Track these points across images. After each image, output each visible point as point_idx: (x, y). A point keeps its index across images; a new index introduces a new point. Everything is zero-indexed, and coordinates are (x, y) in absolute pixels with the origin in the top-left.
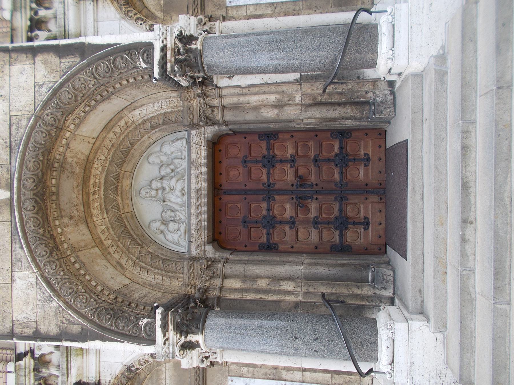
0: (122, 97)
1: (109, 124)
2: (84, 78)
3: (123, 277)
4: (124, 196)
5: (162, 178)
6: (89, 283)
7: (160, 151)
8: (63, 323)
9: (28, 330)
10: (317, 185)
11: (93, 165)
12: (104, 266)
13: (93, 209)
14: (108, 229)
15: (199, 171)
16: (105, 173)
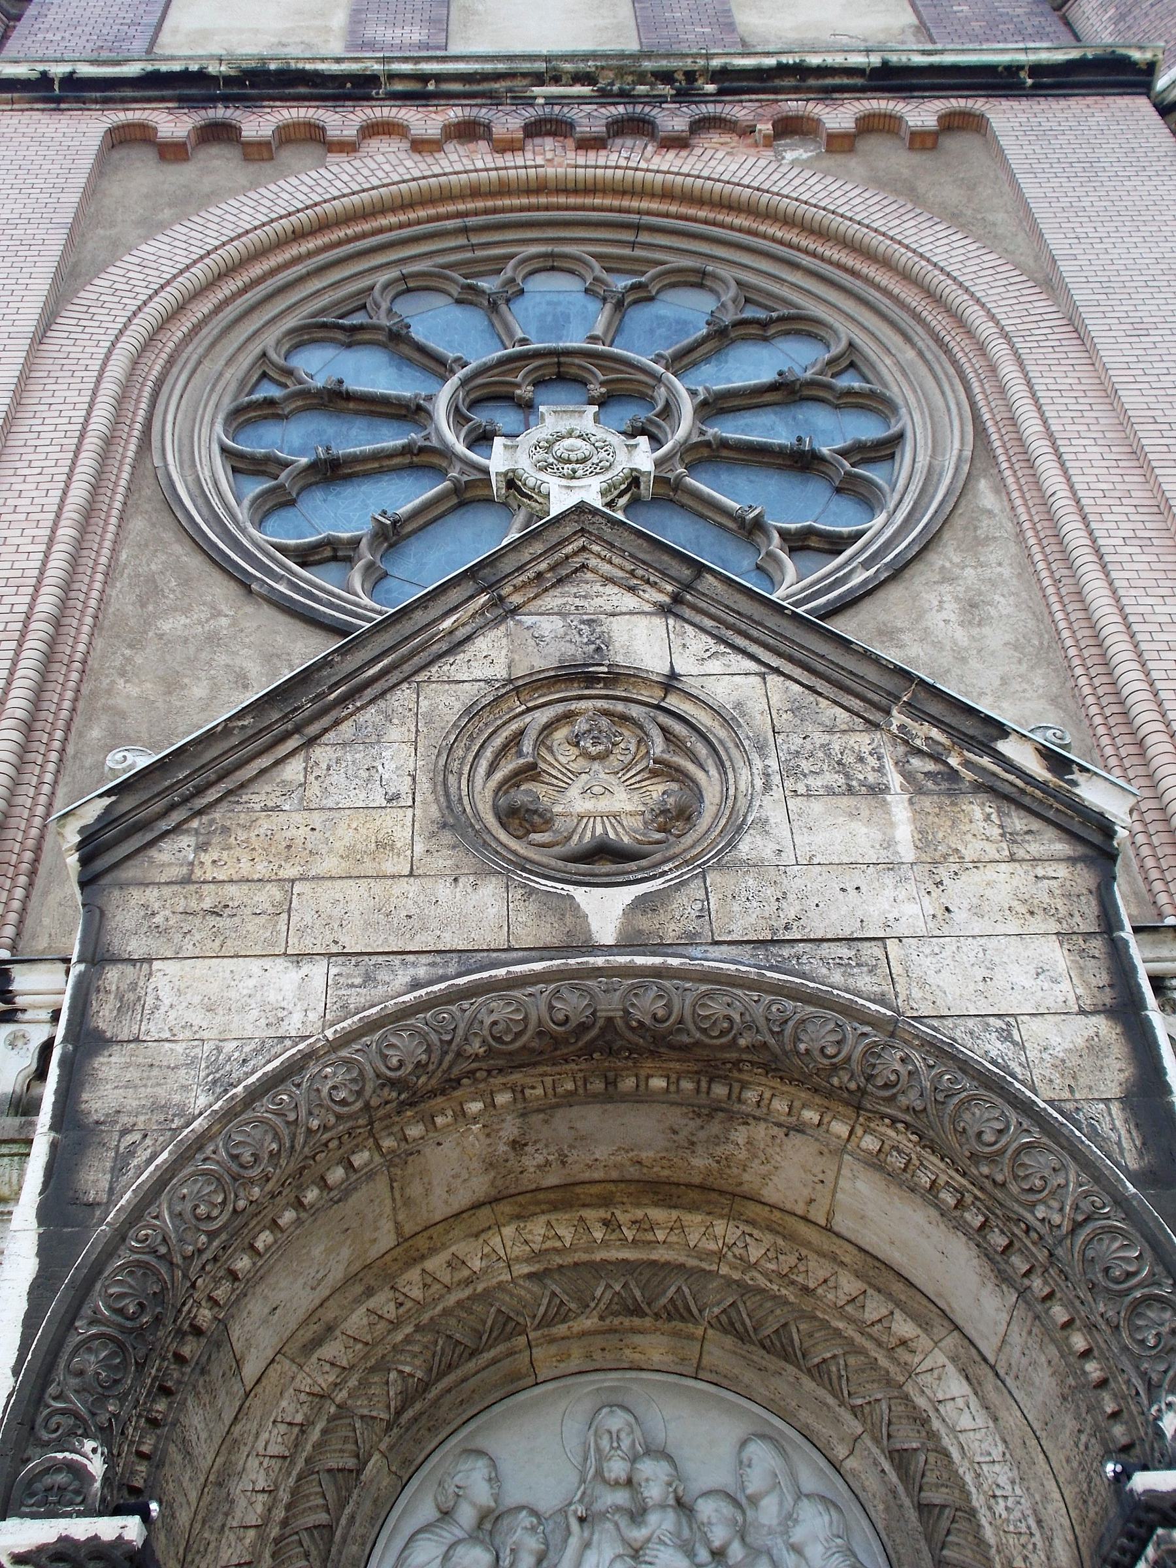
0: (1015, 1327)
1: (891, 1276)
2: (1067, 1185)
3: (270, 1353)
4: (599, 1341)
5: (683, 1506)
6: (267, 1221)
7: (799, 1495)
8: (125, 1132)
9: (111, 1011)
11: (722, 1217)
12: (319, 1276)
13: (549, 1223)
14: (468, 1282)
16: (692, 1262)
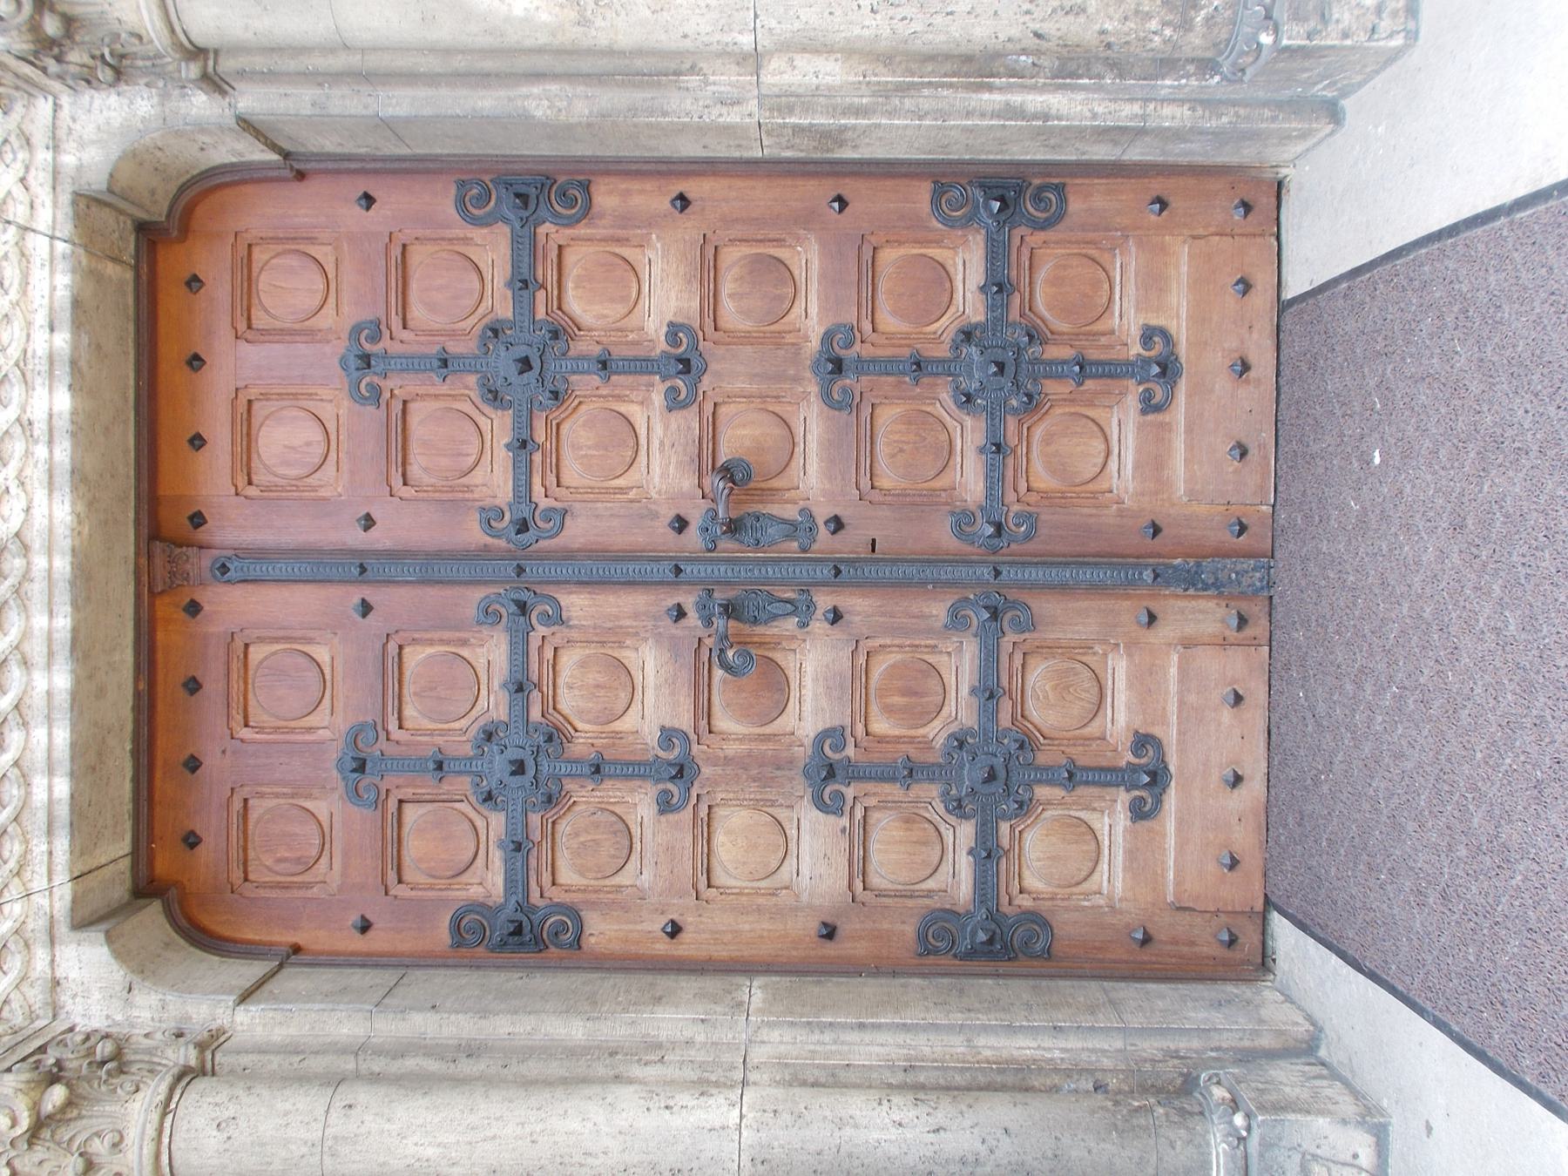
10: (837, 524)
15: (12, 413)
